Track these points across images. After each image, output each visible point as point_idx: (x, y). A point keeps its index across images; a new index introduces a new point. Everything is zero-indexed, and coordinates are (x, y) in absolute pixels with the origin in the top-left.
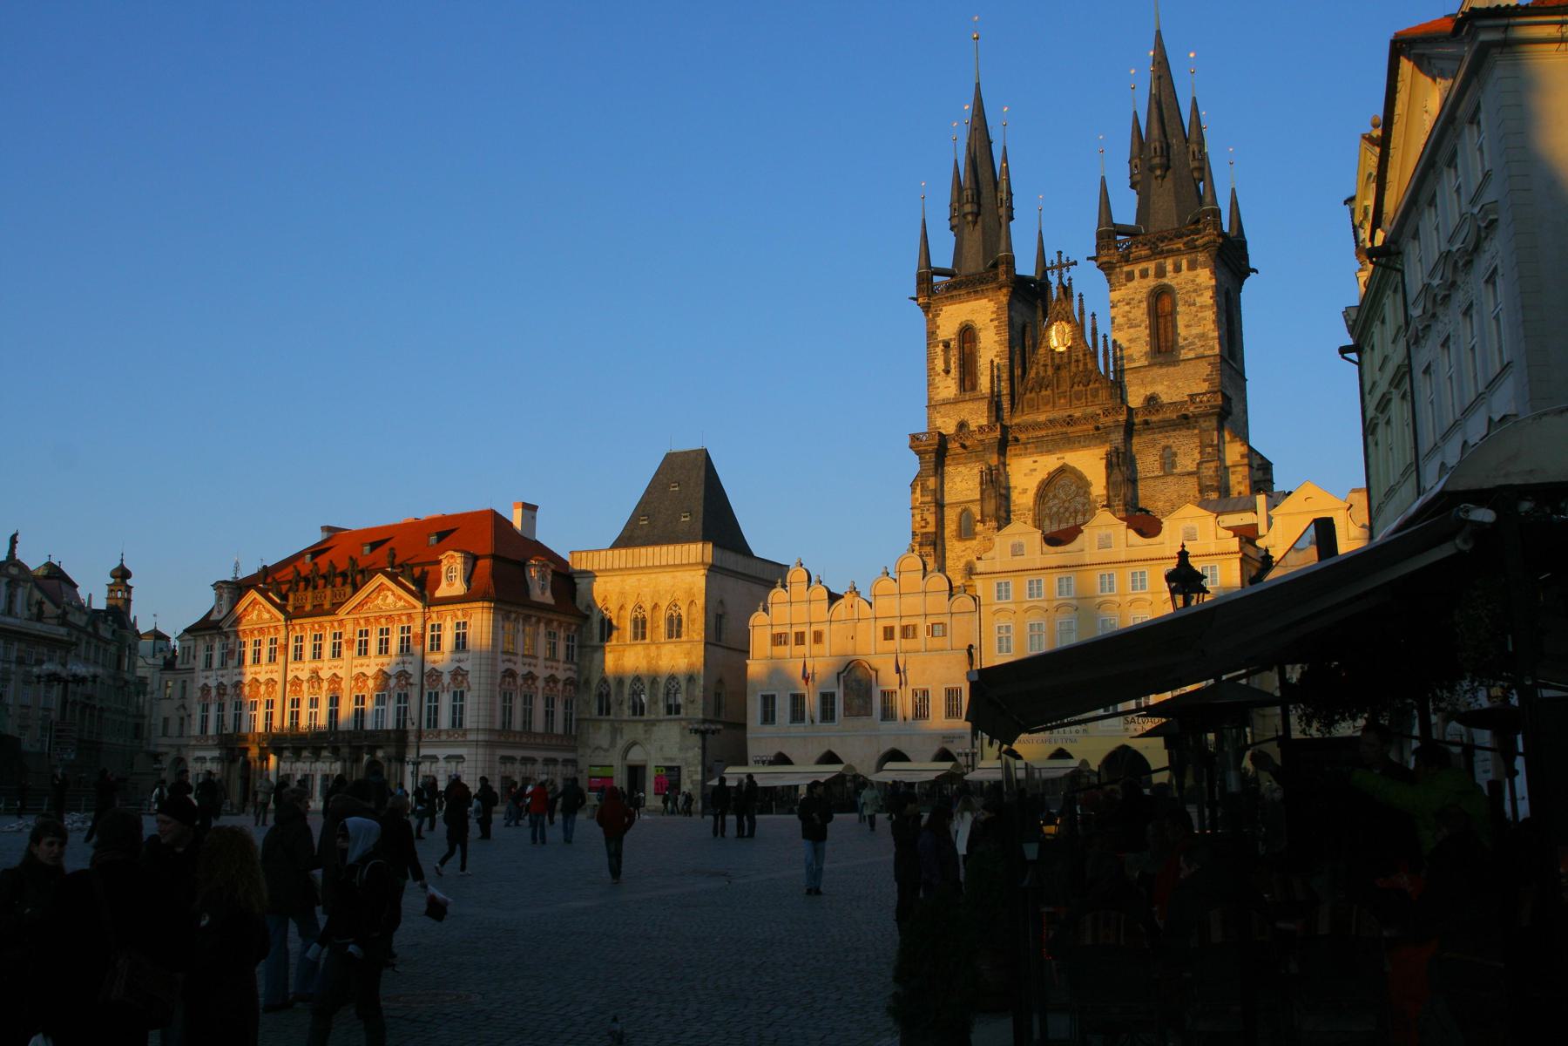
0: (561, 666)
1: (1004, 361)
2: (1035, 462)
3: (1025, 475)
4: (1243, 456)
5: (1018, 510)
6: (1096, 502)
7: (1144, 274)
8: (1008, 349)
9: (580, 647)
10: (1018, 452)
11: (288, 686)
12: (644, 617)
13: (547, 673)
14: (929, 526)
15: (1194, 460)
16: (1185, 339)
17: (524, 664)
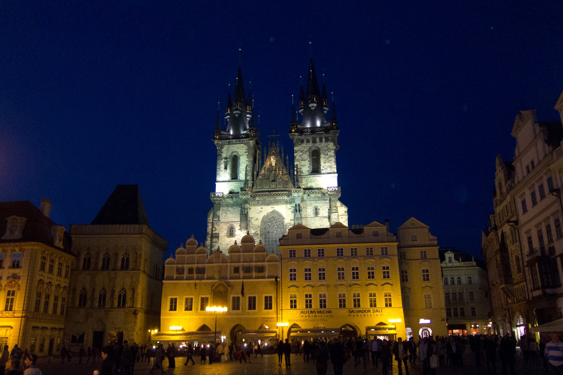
0: (63, 280)
1: (250, 168)
2: (262, 208)
3: (258, 213)
4: (345, 212)
5: (254, 227)
6: (287, 225)
7: (308, 141)
8: (252, 164)
9: (71, 271)
10: (254, 204)
12: (108, 258)
13: (57, 283)
14: (216, 230)
16: (323, 167)
17: (48, 278)
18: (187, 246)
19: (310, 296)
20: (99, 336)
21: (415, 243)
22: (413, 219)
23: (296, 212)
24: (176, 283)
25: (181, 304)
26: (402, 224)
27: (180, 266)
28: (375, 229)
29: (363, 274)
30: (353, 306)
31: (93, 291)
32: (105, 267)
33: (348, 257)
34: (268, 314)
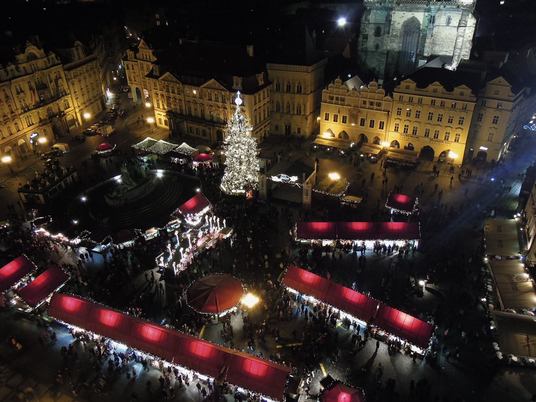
2: (404, 14)
3: (400, 18)
4: (474, 24)
6: (421, 31)
9: (270, 91)
10: (398, 9)
11: (186, 103)
12: (289, 85)
15: (457, 22)
18: (335, 83)
19: (408, 126)
20: (288, 128)
21: (496, 96)
22: (501, 78)
23: (430, 23)
24: (328, 105)
25: (331, 117)
26: (490, 81)
27: (331, 95)
28: (462, 90)
29: (445, 120)
30: (433, 138)
31: (283, 103)
32: (288, 90)
33: (438, 106)
34: (381, 131)
